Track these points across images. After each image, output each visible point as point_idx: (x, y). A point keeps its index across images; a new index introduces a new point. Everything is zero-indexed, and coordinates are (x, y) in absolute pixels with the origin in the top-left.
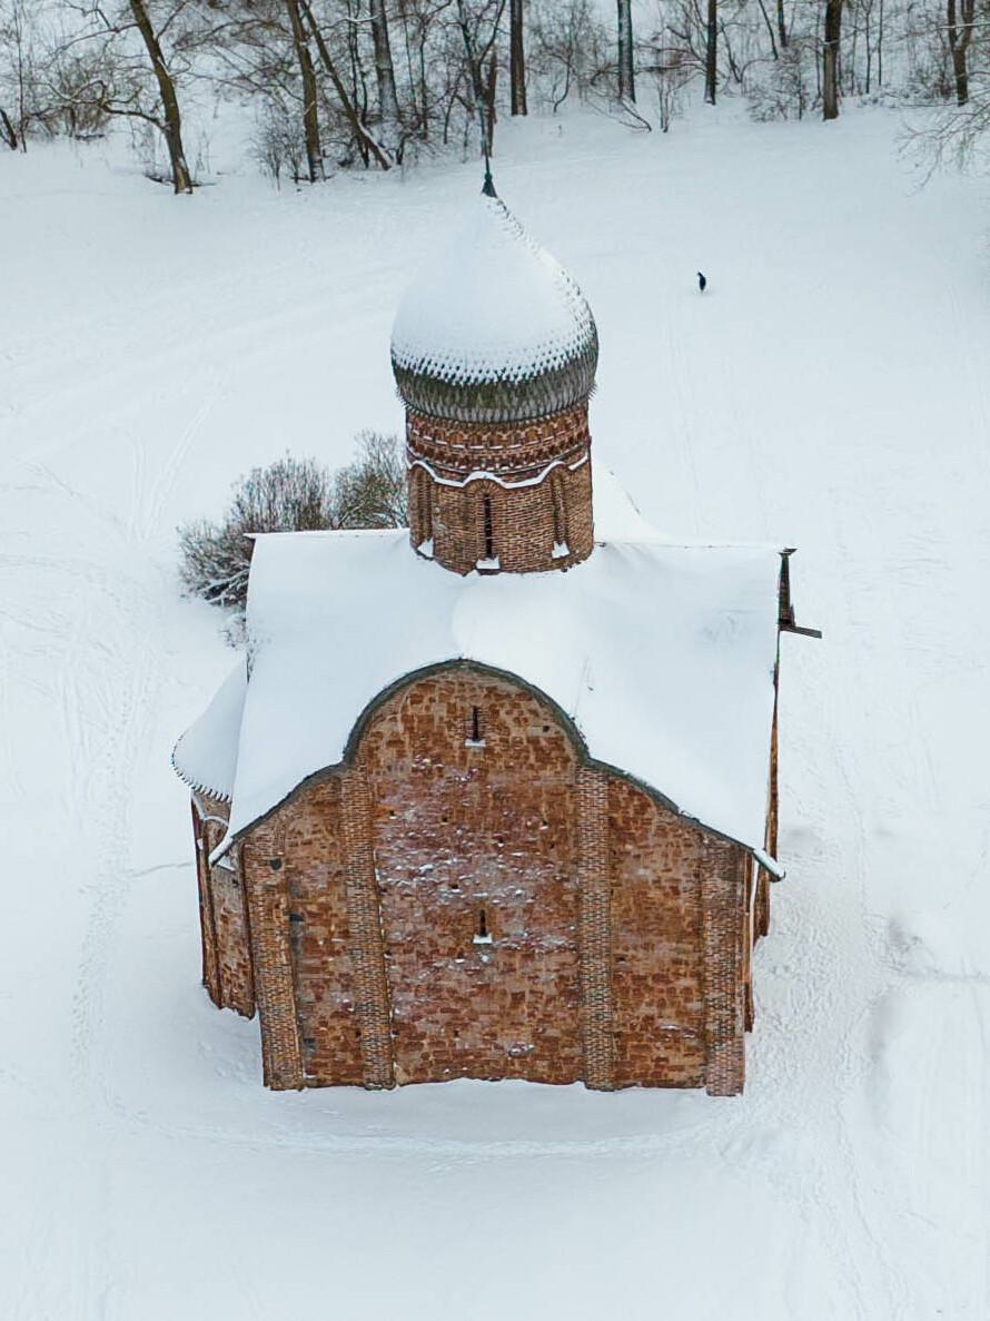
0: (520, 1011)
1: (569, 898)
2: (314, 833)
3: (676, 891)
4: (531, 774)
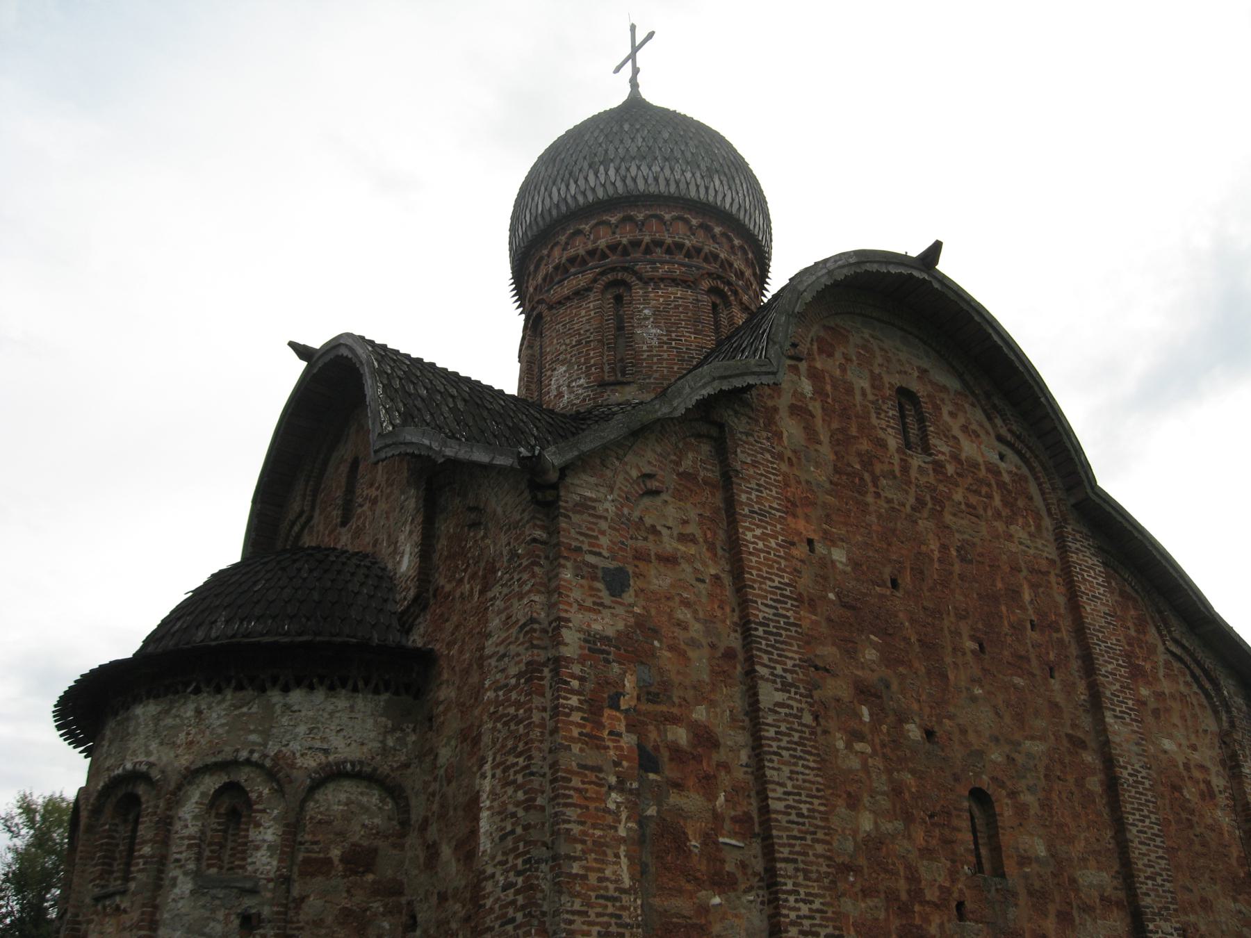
1: (1094, 783)
2: (683, 538)
3: (1209, 794)
4: (1000, 526)
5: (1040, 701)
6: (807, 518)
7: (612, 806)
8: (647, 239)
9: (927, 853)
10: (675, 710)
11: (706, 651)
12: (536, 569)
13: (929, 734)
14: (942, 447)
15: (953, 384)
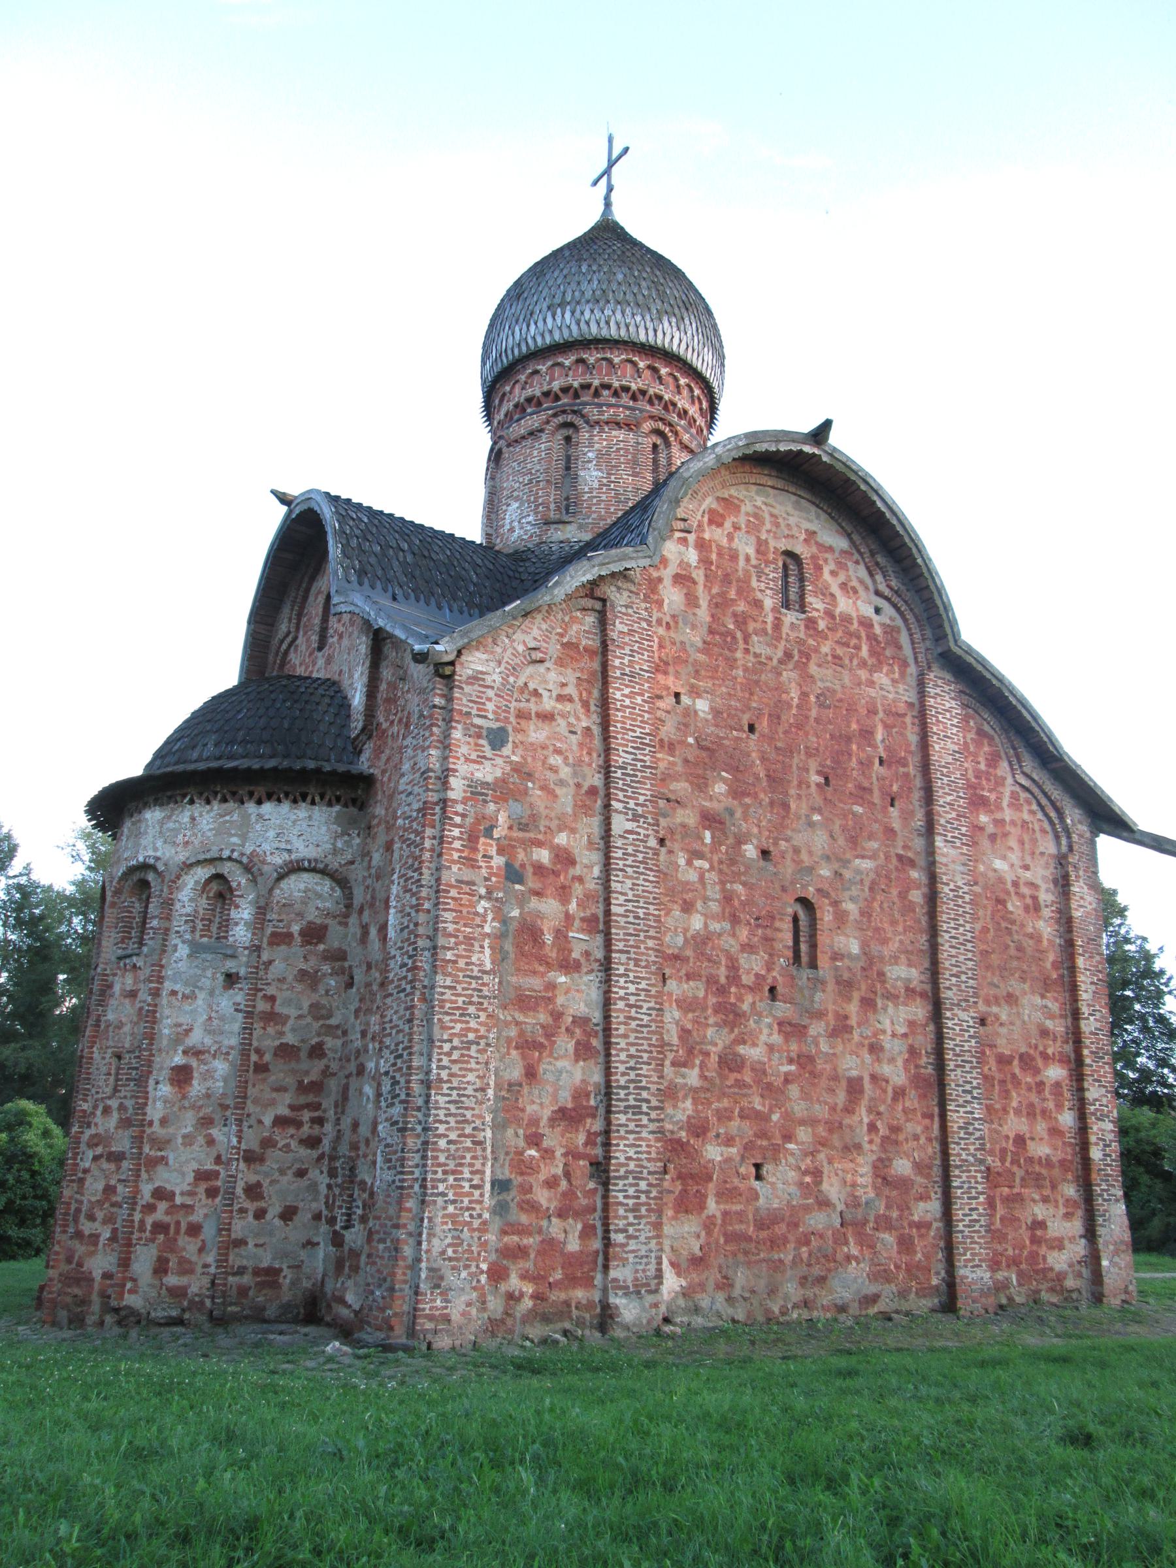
0: (856, 1118)
1: (917, 896)
2: (560, 698)
3: (1035, 907)
4: (863, 674)
5: (876, 826)
6: (677, 675)
7: (480, 910)
8: (596, 383)
9: (748, 948)
10: (540, 837)
11: (572, 790)
12: (435, 729)
13: (765, 854)
14: (816, 603)
15: (842, 543)
